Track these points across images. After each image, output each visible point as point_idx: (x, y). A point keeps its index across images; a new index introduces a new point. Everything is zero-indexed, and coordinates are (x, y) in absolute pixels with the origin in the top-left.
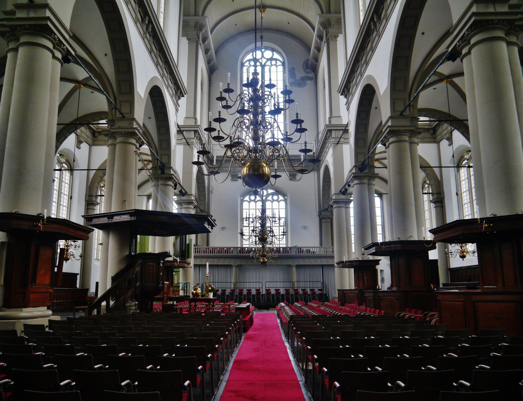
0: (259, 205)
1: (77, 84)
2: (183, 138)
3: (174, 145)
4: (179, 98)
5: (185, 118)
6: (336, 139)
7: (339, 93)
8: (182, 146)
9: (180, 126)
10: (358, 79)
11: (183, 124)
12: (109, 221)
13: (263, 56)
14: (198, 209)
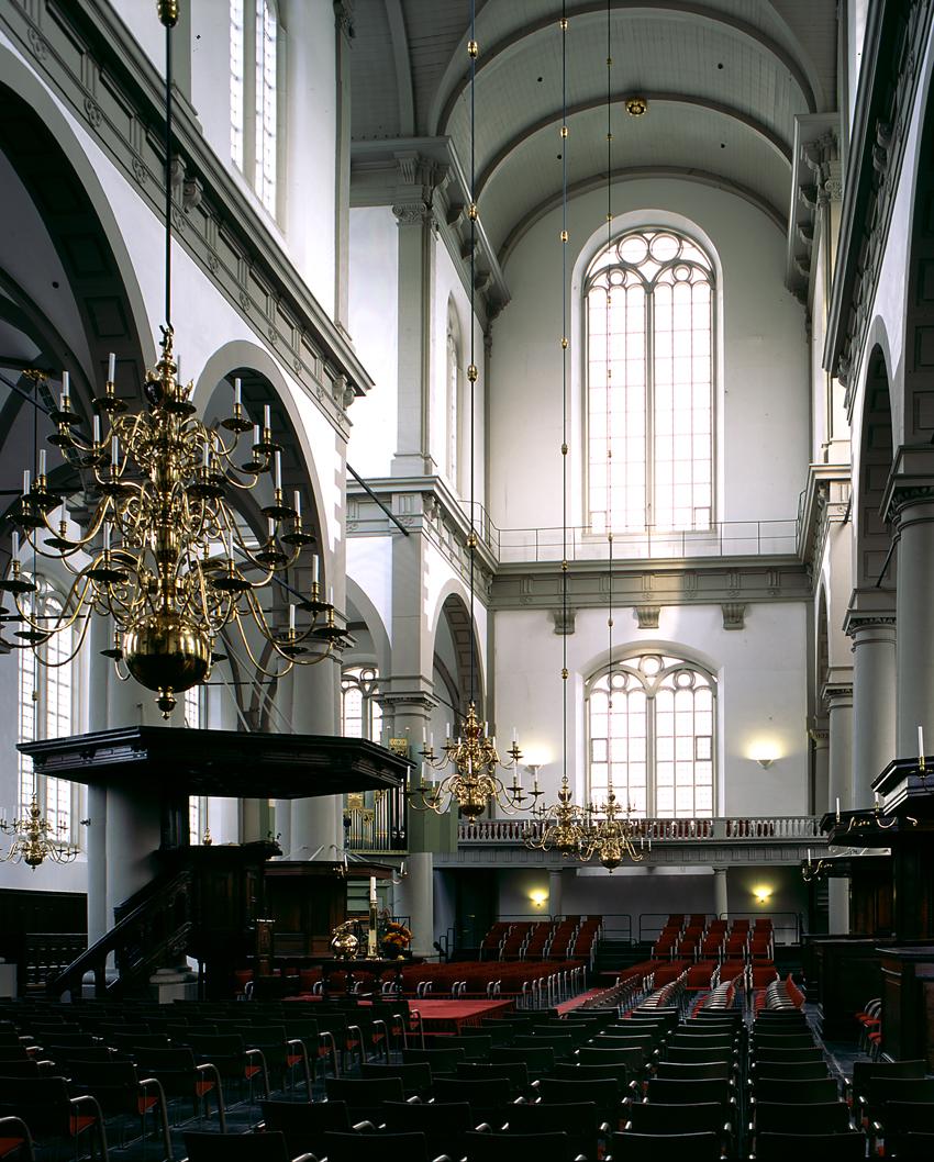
0: (639, 700)
4: (348, 402)
5: (395, 455)
11: (387, 474)
12: (135, 756)
13: (649, 257)
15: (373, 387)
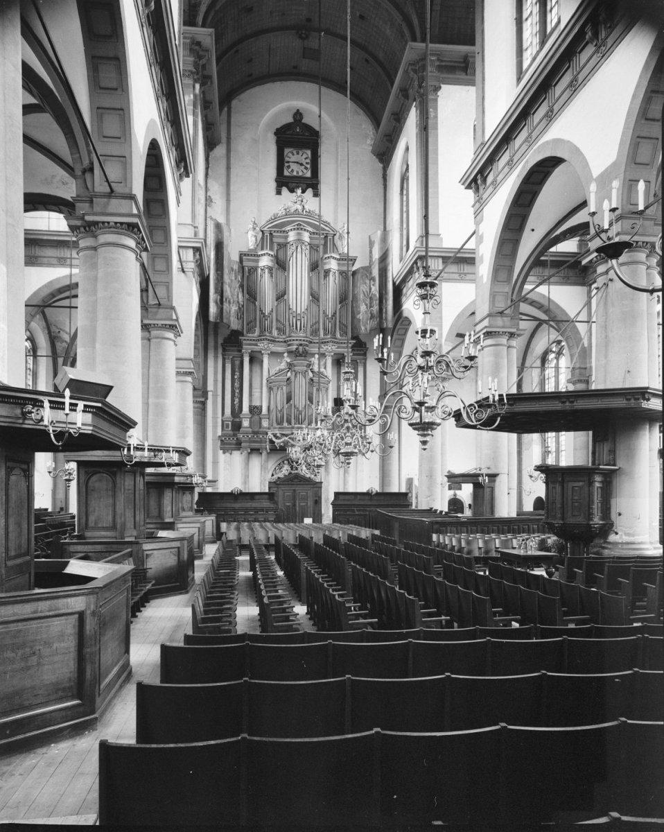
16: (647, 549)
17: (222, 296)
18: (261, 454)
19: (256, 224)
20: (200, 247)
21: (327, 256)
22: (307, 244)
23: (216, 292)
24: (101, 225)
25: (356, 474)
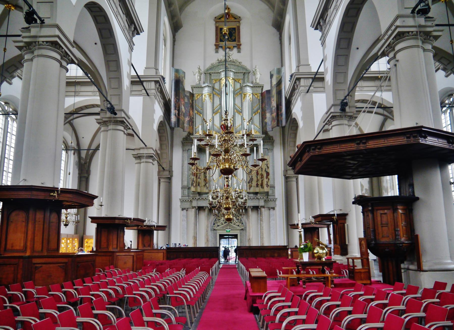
1: (6, 5)
2: (143, 88)
3: (127, 86)
5: (145, 68)
6: (306, 87)
7: (313, 27)
8: (141, 98)
9: (140, 77)
10: (326, 29)
14: (161, 167)
15: (143, 32)
16: (449, 264)
17: (179, 111)
18: (204, 210)
19: (200, 69)
20: (159, 81)
21: (244, 85)
22: (232, 79)
23: (175, 109)
24: (34, 44)
25: (270, 222)
